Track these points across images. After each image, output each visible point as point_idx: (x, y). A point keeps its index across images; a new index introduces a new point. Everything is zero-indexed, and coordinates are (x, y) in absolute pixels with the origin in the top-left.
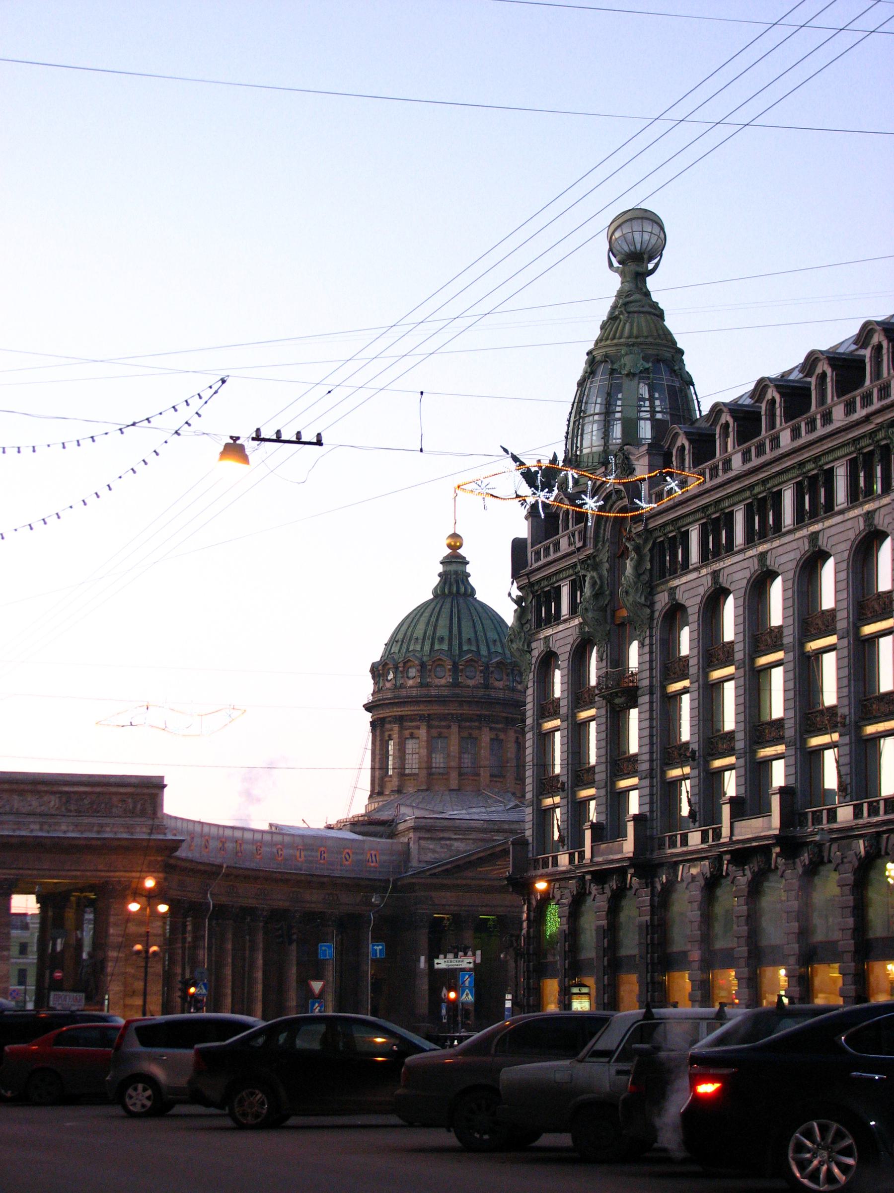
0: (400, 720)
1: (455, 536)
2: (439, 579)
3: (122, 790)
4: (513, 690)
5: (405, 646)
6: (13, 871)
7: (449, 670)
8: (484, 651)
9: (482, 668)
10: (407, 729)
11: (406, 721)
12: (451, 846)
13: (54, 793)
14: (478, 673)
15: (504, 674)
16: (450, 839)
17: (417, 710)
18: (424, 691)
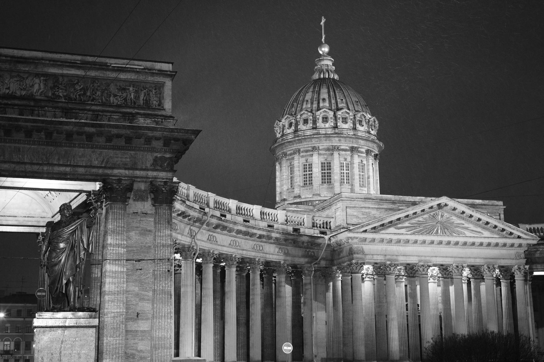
3: (122, 76)
10: (303, 157)
11: (302, 152)
14: (349, 121)
16: (369, 208)
17: (311, 144)
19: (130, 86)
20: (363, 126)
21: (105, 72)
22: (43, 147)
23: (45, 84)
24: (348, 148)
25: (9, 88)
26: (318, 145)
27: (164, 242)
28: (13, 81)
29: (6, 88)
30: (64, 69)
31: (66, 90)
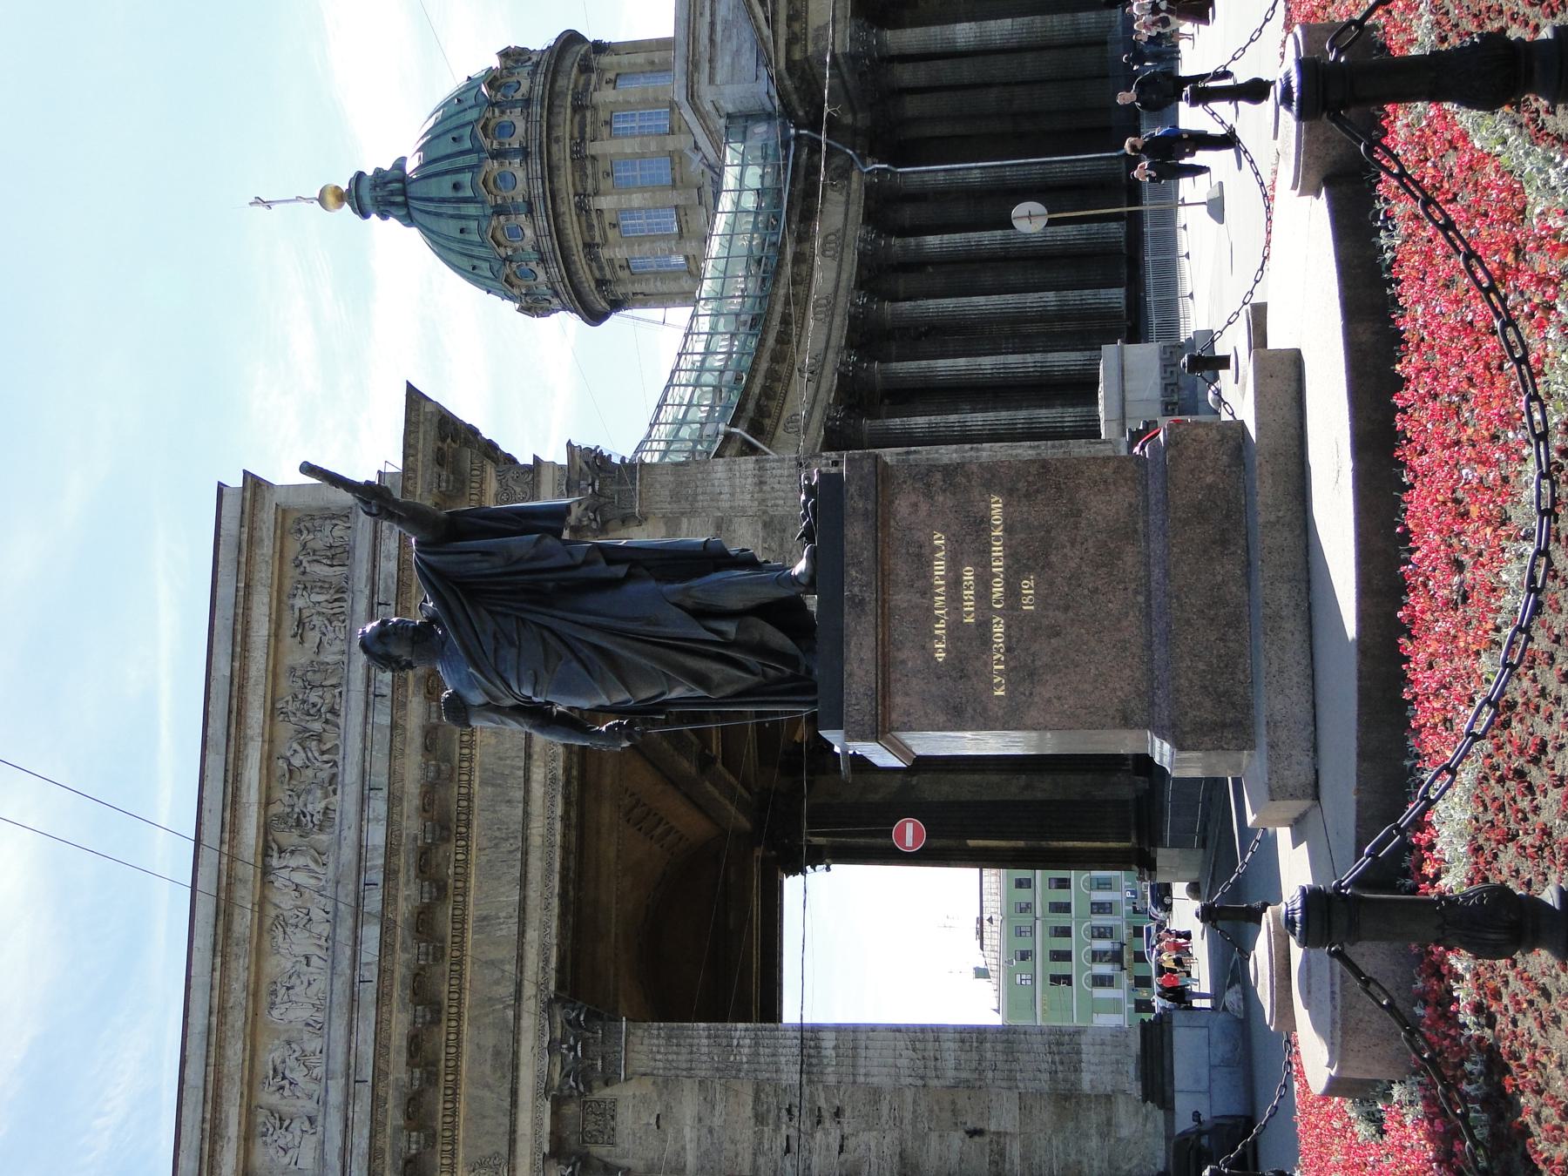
0: (589, 246)
1: (321, 200)
2: (391, 219)
3: (261, 629)
4: (537, 64)
5: (477, 251)
6: (528, 1022)
7: (501, 164)
8: (472, 115)
9: (497, 111)
10: (605, 232)
11: (593, 238)
12: (726, 21)
13: (266, 871)
14: (505, 118)
15: (509, 80)
16: (712, 24)
18: (539, 206)
19: (293, 606)
20: (519, 82)
21: (252, 681)
22: (474, 852)
23: (292, 852)
24: (577, 118)
25: (307, 958)
26: (571, 197)
27: (749, 481)
28: (286, 946)
29: (308, 965)
30: (244, 800)
31: (309, 792)
